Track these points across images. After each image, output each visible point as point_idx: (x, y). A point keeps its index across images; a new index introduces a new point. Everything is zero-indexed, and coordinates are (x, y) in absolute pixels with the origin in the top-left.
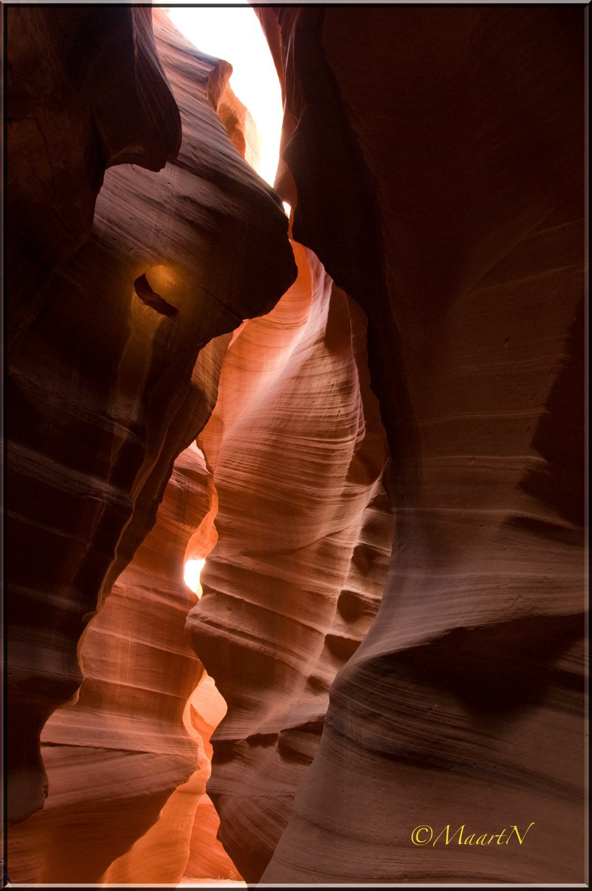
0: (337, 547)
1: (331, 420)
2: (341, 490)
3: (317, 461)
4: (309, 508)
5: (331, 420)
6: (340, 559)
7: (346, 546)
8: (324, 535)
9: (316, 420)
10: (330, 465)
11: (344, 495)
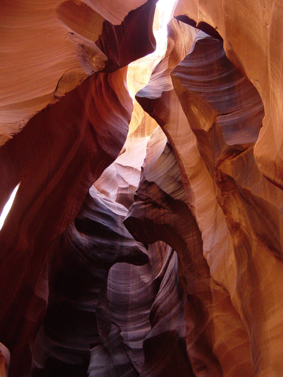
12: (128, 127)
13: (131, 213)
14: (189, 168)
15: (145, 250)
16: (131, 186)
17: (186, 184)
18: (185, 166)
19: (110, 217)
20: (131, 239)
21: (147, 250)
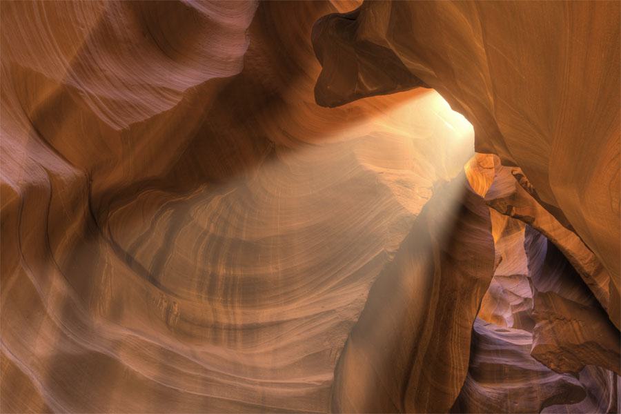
12: (492, 236)
13: (536, 340)
14: (588, 263)
15: (575, 379)
16: (526, 299)
17: (592, 284)
18: (581, 263)
19: (515, 353)
20: (549, 372)
21: (578, 379)
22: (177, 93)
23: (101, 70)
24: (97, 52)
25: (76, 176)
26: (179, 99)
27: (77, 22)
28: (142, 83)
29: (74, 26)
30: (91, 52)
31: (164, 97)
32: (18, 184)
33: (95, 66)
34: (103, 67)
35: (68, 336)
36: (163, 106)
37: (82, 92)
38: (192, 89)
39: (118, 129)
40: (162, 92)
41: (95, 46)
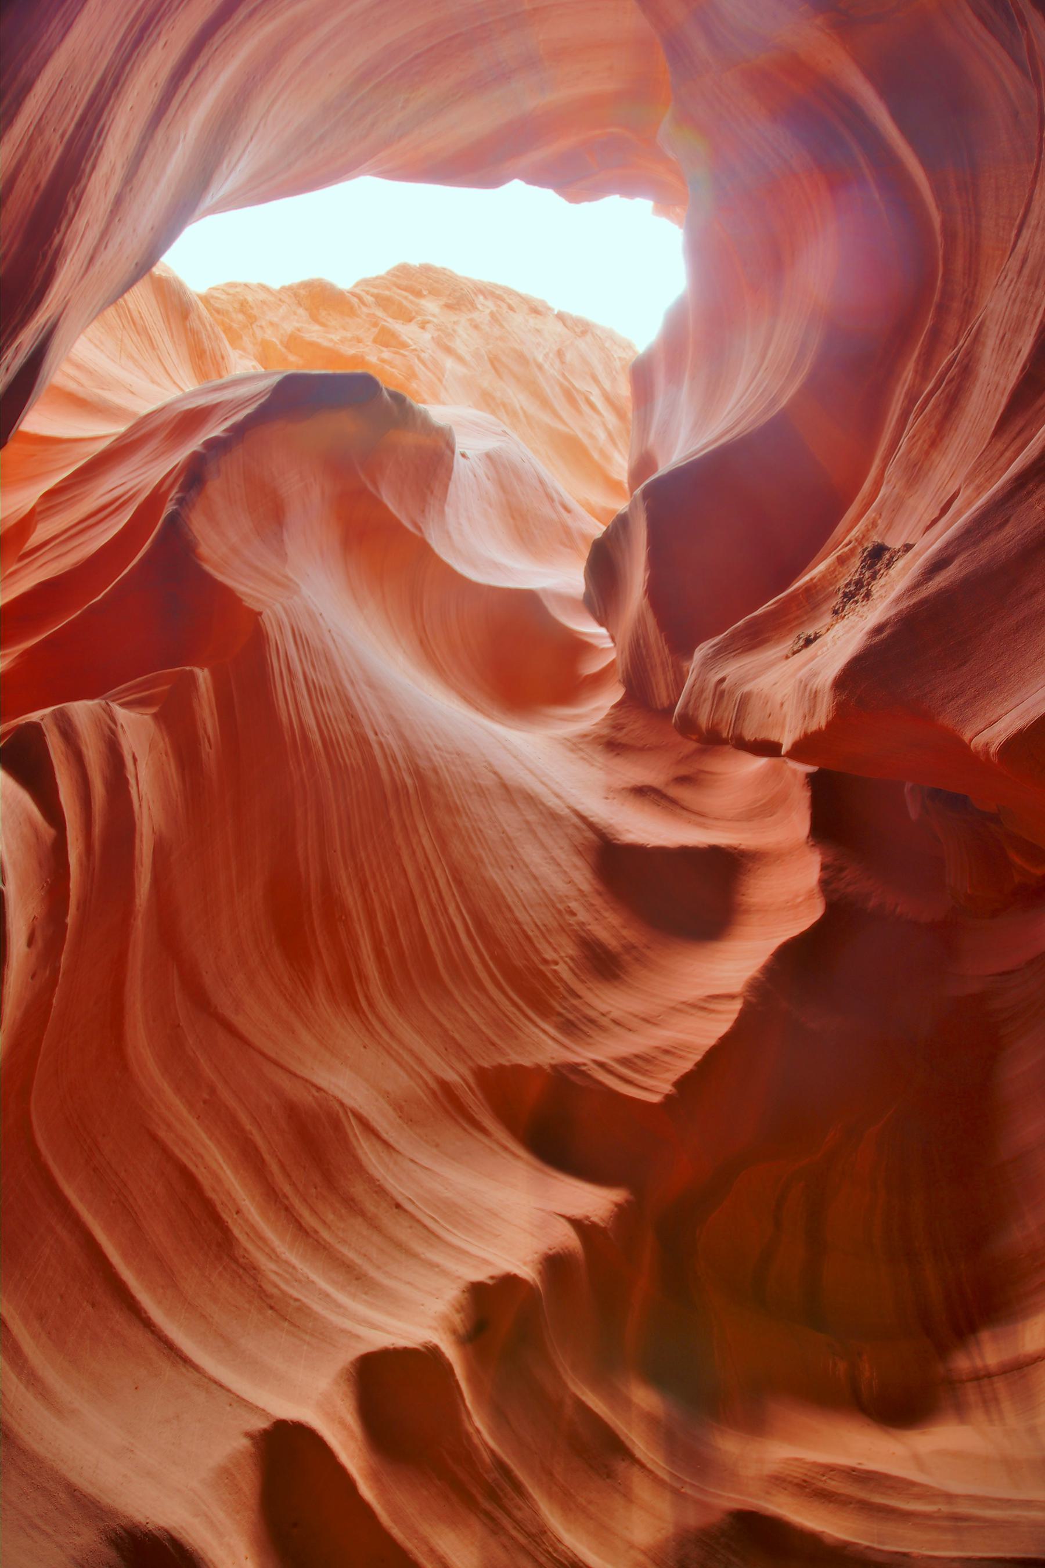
0: (360, 1168)
1: (527, 947)
2: (451, 1076)
3: (432, 941)
4: (329, 985)
5: (527, 947)
6: (352, 1206)
7: (409, 1207)
8: (349, 1102)
9: (499, 902)
10: (449, 993)
11: (443, 1084)
22: (731, 997)
23: (603, 1015)
24: (589, 989)
25: (617, 1205)
26: (737, 1005)
27: (545, 962)
28: (672, 1004)
29: (543, 967)
30: (580, 993)
31: (713, 1011)
32: (525, 1264)
33: (592, 1014)
34: (603, 1007)
35: (683, 1490)
36: (715, 1027)
37: (585, 1064)
38: (754, 979)
39: (655, 1099)
40: (706, 1005)
41: (583, 982)
